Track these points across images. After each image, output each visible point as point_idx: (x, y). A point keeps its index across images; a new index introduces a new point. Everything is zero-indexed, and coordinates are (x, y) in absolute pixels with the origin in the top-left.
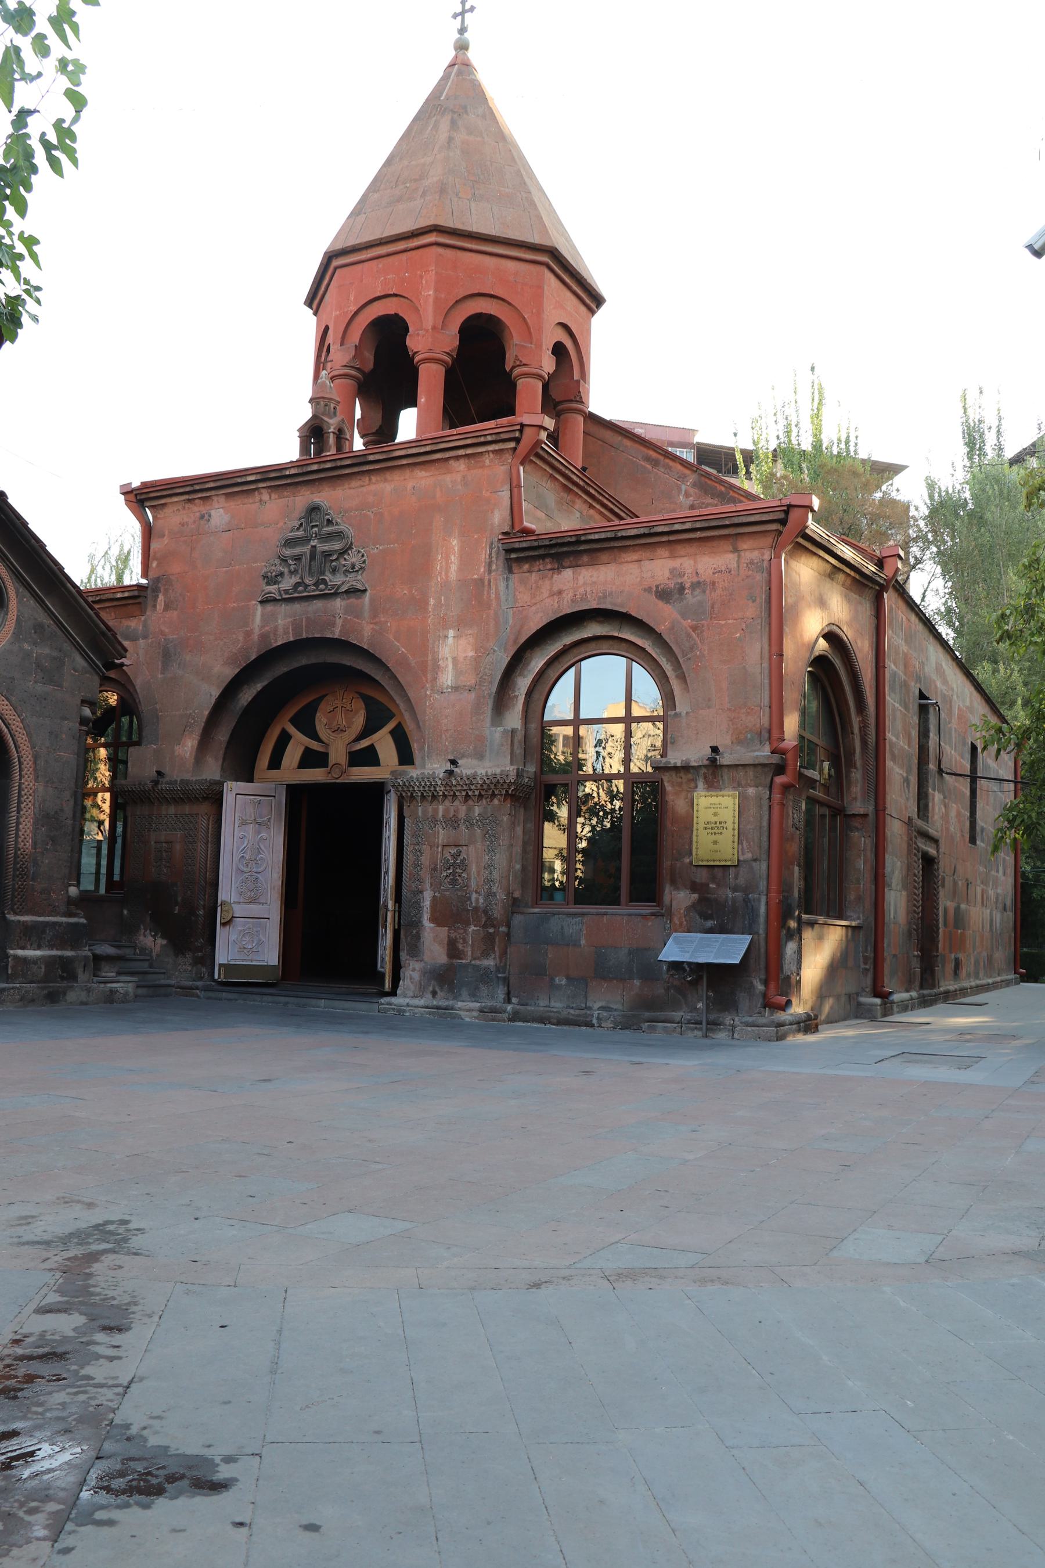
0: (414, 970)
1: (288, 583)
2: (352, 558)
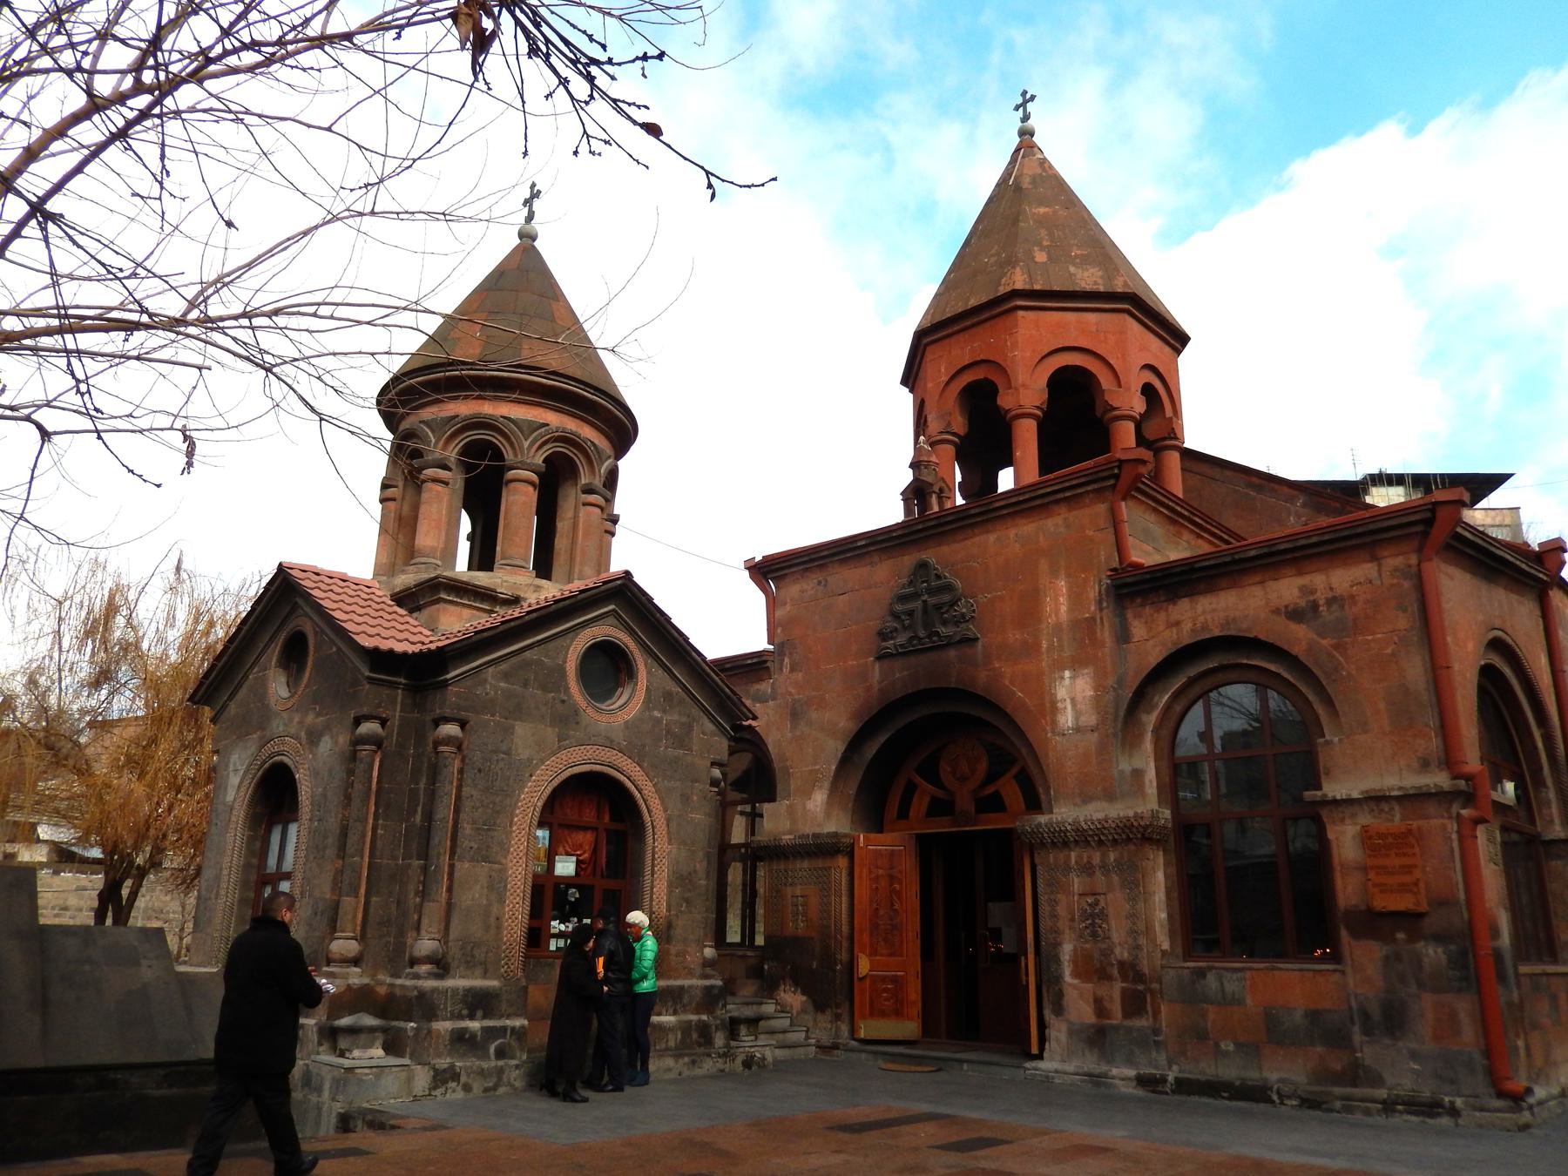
0: (1059, 1031)
1: (902, 639)
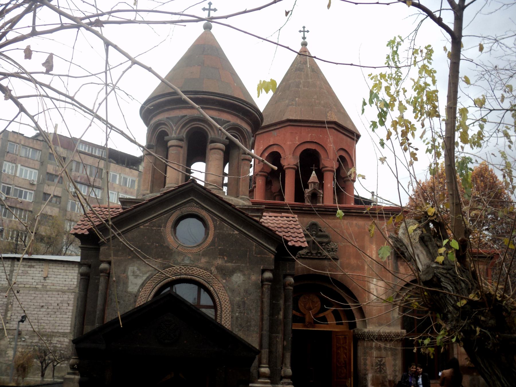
2: (332, 246)
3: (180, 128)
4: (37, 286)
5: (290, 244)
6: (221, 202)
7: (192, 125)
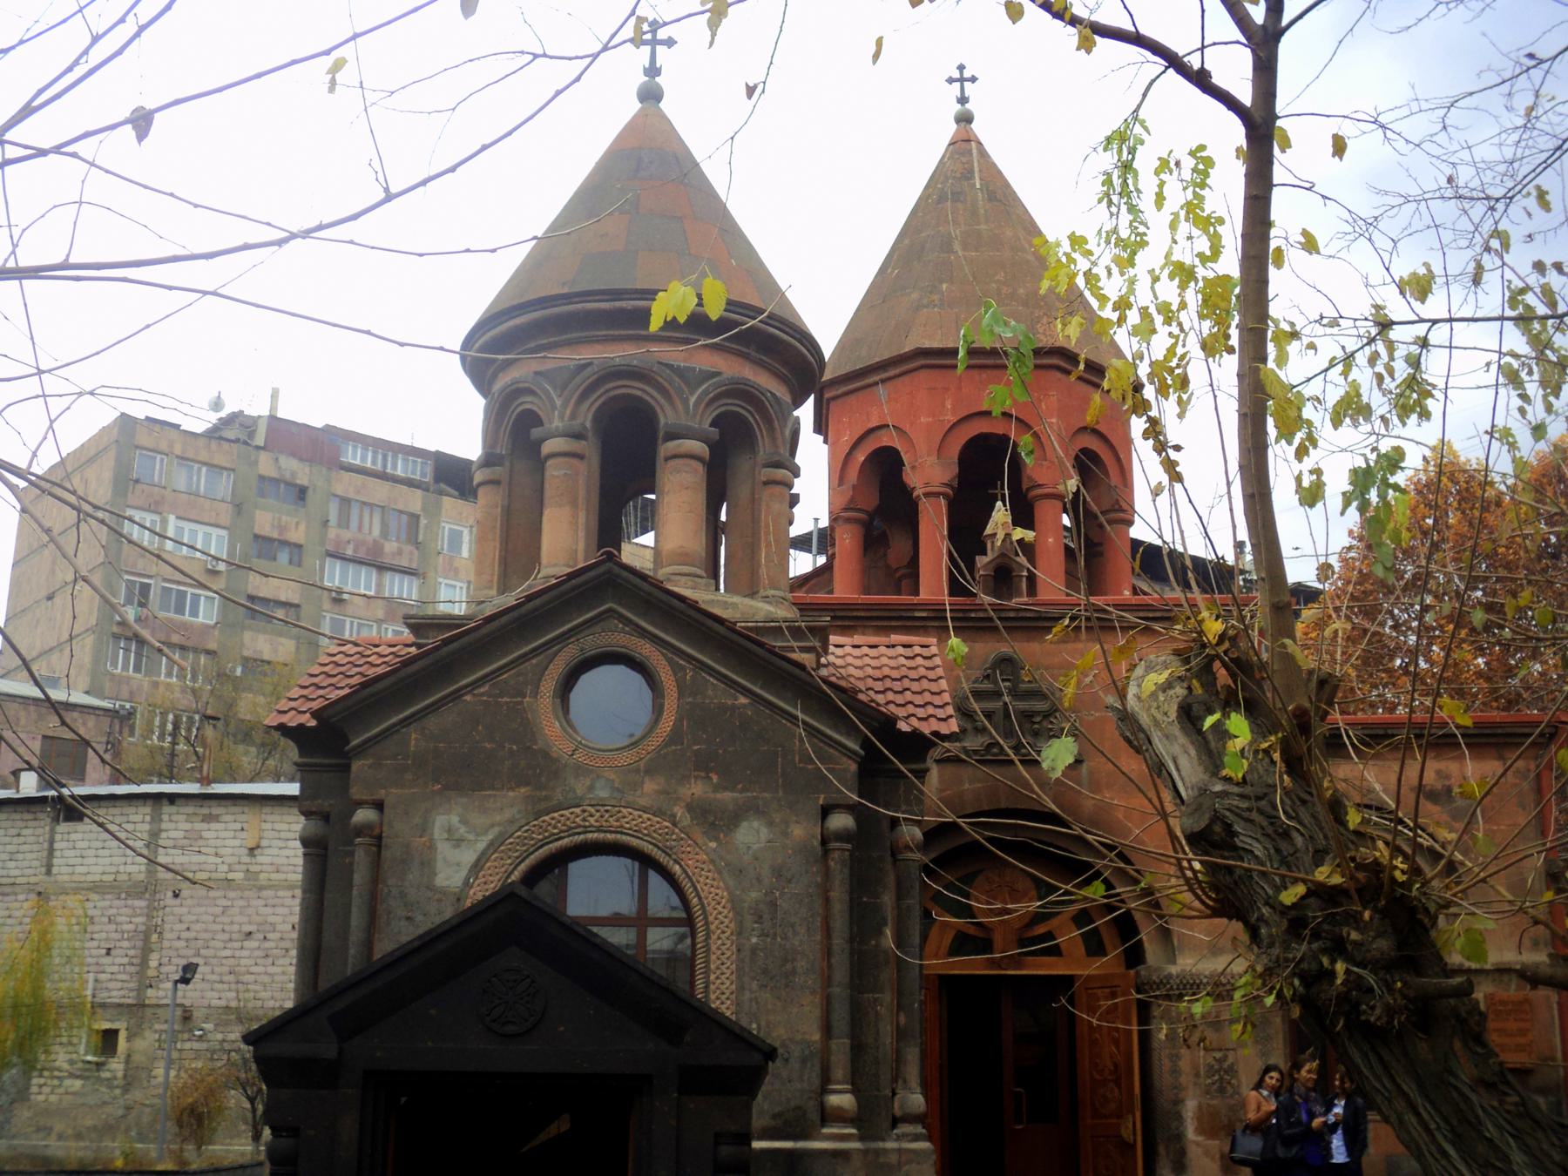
3: (573, 401)
4: (230, 876)
5: (903, 726)
6: (693, 613)
7: (607, 391)
